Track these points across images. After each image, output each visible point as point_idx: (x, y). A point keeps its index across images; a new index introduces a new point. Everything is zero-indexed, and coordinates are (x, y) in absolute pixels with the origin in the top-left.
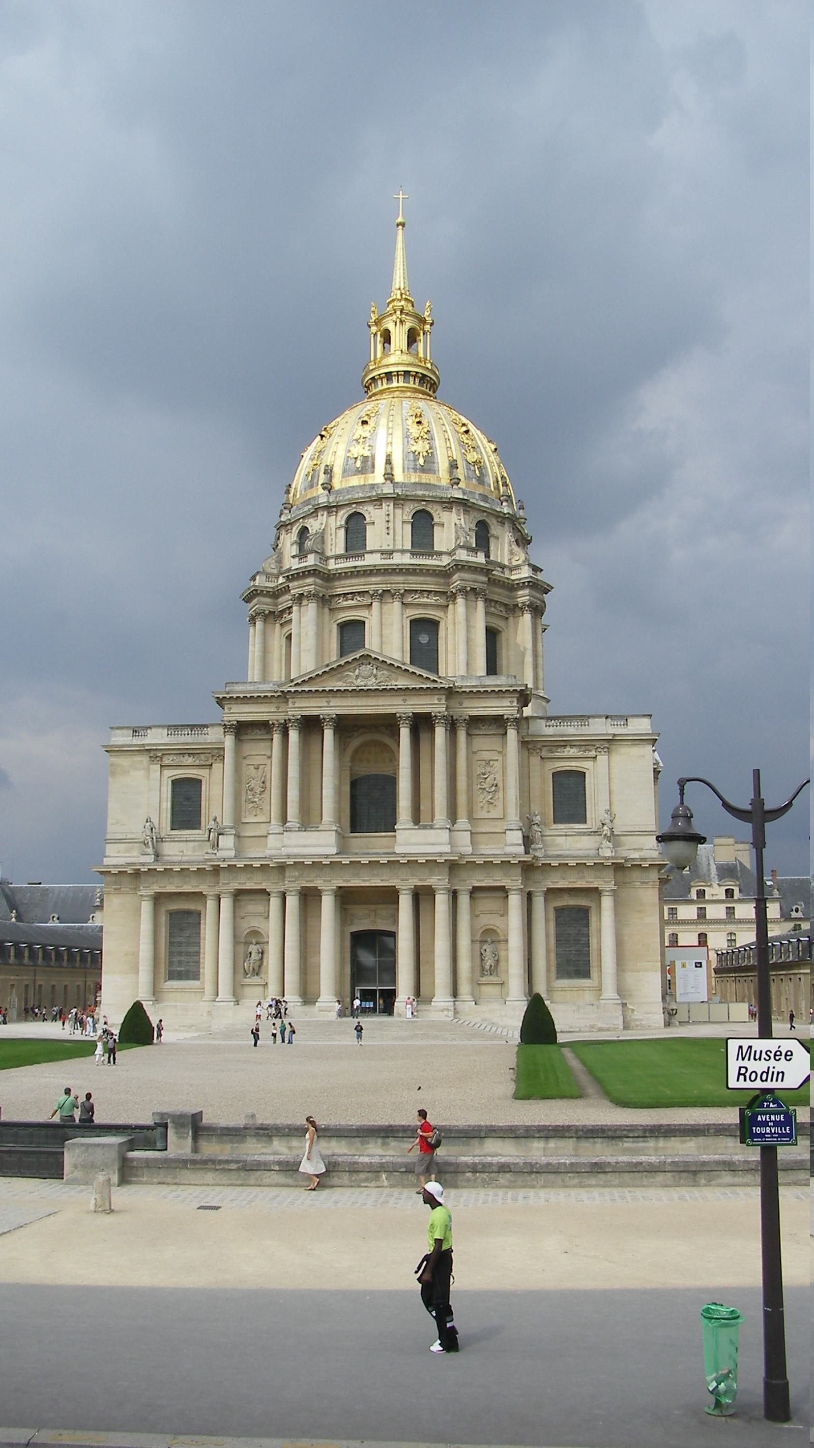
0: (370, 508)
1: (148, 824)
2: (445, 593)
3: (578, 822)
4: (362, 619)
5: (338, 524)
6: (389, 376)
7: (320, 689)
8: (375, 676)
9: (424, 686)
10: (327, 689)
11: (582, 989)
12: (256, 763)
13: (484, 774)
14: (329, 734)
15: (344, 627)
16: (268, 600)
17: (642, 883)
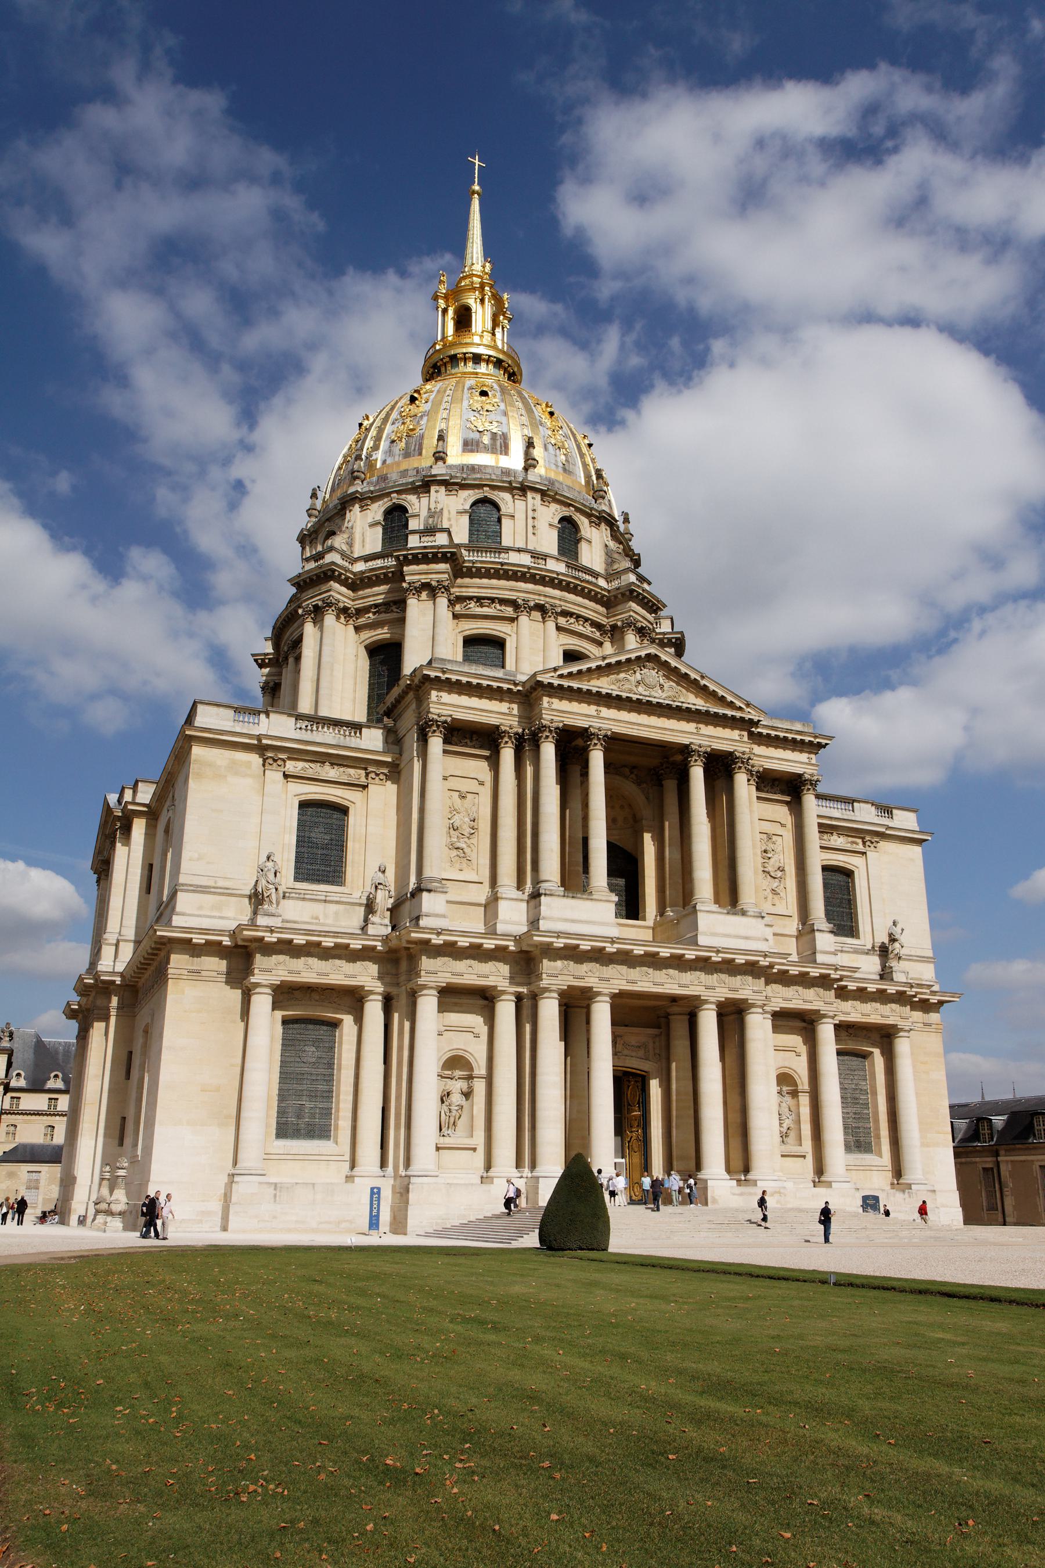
0: (507, 496)
1: (270, 864)
2: (598, 626)
3: (846, 936)
4: (501, 635)
5: (461, 508)
6: (477, 359)
7: (594, 690)
8: (662, 687)
9: (730, 713)
10: (604, 691)
11: (868, 1168)
12: (464, 789)
13: (765, 851)
14: (597, 759)
15: (470, 642)
16: (343, 590)
17: (925, 1024)
